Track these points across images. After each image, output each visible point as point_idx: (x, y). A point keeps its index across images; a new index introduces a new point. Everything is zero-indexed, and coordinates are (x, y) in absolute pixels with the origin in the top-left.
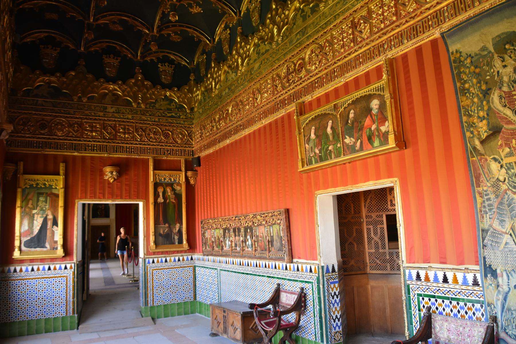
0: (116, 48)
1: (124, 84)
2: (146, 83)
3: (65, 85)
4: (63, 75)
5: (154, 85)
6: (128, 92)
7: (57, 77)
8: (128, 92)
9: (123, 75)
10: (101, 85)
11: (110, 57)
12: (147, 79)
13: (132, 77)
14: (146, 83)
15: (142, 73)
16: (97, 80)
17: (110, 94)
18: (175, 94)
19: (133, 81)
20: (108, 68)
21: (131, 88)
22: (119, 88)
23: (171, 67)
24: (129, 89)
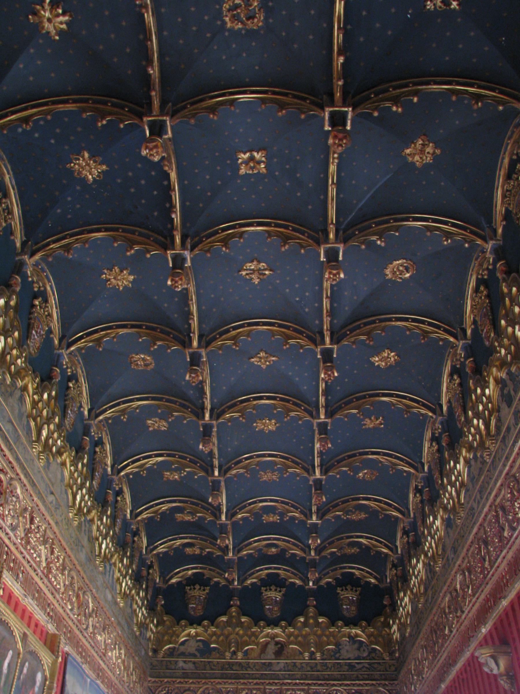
0: (278, 575)
1: (290, 626)
2: (320, 620)
3: (214, 638)
4: (212, 623)
5: (333, 623)
6: (296, 637)
7: (204, 627)
8: (296, 637)
9: (288, 615)
10: (262, 631)
11: (271, 590)
12: (321, 614)
13: (301, 614)
14: (320, 620)
15: (314, 606)
16: (256, 625)
17: (273, 643)
18: (363, 631)
19: (302, 620)
20: (269, 605)
21: (300, 630)
22: (284, 632)
23: (356, 591)
24: (296, 632)
